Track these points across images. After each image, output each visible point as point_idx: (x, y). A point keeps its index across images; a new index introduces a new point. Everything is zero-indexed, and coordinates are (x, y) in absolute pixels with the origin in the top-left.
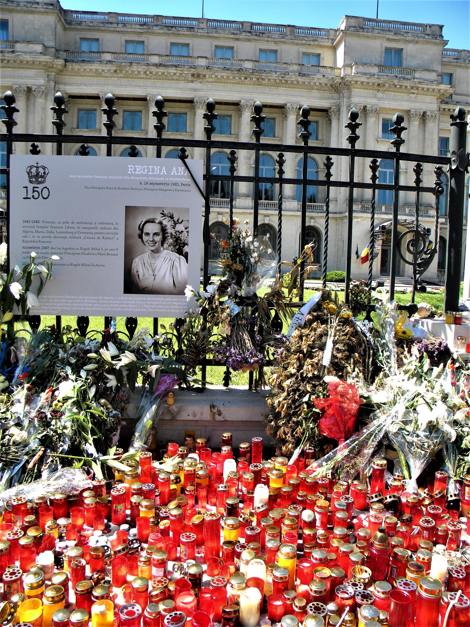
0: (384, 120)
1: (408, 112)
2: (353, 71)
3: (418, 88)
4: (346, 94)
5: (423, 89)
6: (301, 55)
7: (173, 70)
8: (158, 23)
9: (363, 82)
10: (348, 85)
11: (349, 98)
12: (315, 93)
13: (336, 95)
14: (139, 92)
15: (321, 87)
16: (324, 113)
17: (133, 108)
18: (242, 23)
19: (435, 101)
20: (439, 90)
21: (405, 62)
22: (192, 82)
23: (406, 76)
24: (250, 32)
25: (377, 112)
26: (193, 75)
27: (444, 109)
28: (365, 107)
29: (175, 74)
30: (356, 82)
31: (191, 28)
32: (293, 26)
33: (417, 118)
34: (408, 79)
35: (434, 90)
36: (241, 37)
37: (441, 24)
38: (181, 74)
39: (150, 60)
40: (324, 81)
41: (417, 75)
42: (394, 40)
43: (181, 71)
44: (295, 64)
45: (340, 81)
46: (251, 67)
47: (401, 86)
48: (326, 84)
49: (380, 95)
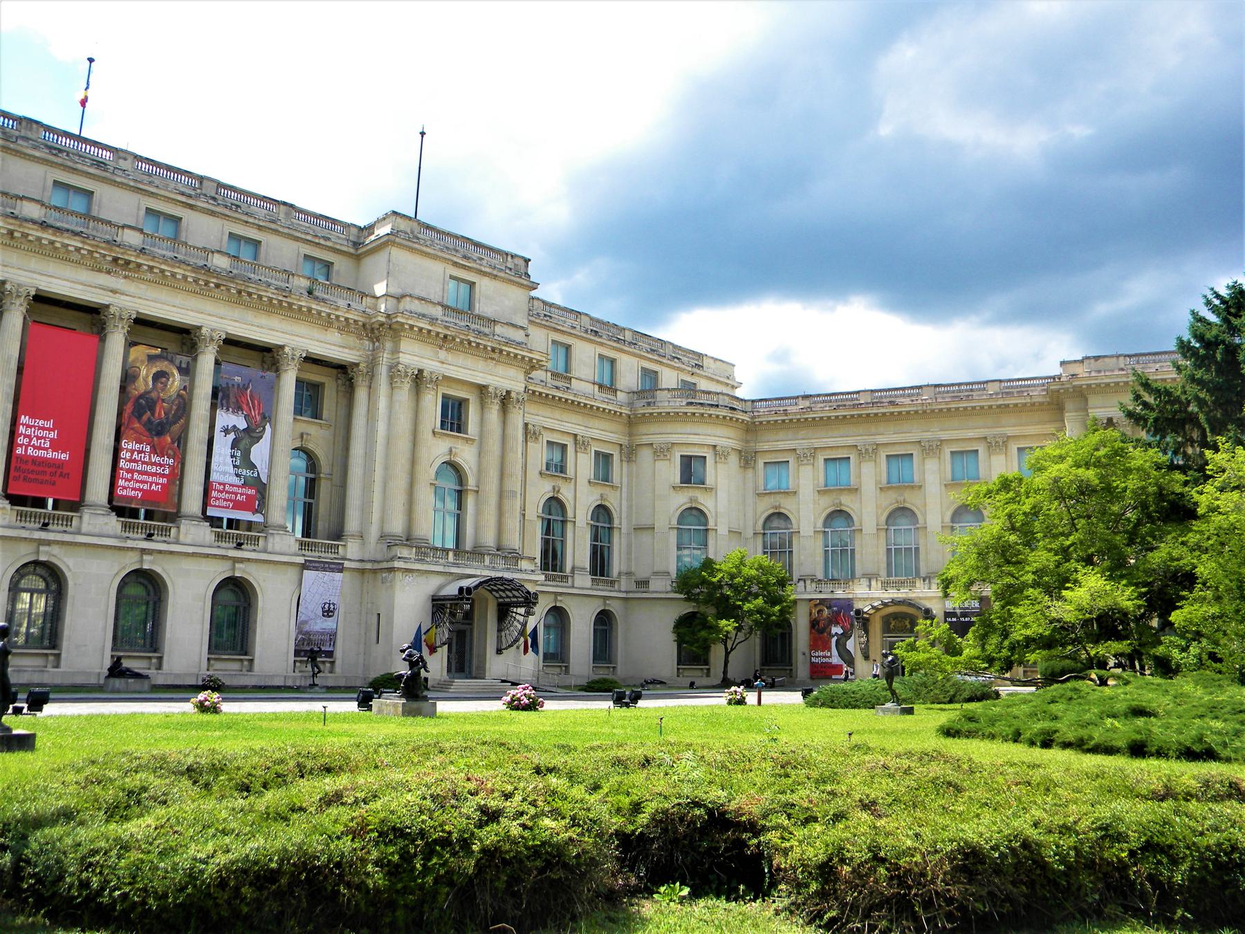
0: (445, 397)
1: (482, 389)
3: (501, 351)
4: (389, 345)
5: (508, 354)
6: (301, 259)
7: (75, 243)
8: (29, 135)
9: (421, 329)
10: (395, 330)
11: (396, 351)
12: (334, 336)
15: (346, 326)
16: (334, 371)
18: (201, 179)
19: (521, 376)
20: (531, 359)
21: (477, 305)
22: (109, 272)
23: (482, 329)
24: (214, 199)
25: (436, 382)
26: (115, 260)
27: (534, 392)
28: (421, 371)
29: (78, 250)
30: (412, 327)
31: (100, 164)
32: (292, 206)
33: (497, 401)
34: (486, 335)
35: (523, 357)
36: (199, 204)
37: (527, 256)
38: (91, 252)
39: (18, 207)
41: (499, 329)
42: (464, 267)
43: (92, 246)
44: (304, 277)
45: (383, 319)
46: (224, 266)
47: (478, 344)
48: (355, 321)
49: (443, 354)
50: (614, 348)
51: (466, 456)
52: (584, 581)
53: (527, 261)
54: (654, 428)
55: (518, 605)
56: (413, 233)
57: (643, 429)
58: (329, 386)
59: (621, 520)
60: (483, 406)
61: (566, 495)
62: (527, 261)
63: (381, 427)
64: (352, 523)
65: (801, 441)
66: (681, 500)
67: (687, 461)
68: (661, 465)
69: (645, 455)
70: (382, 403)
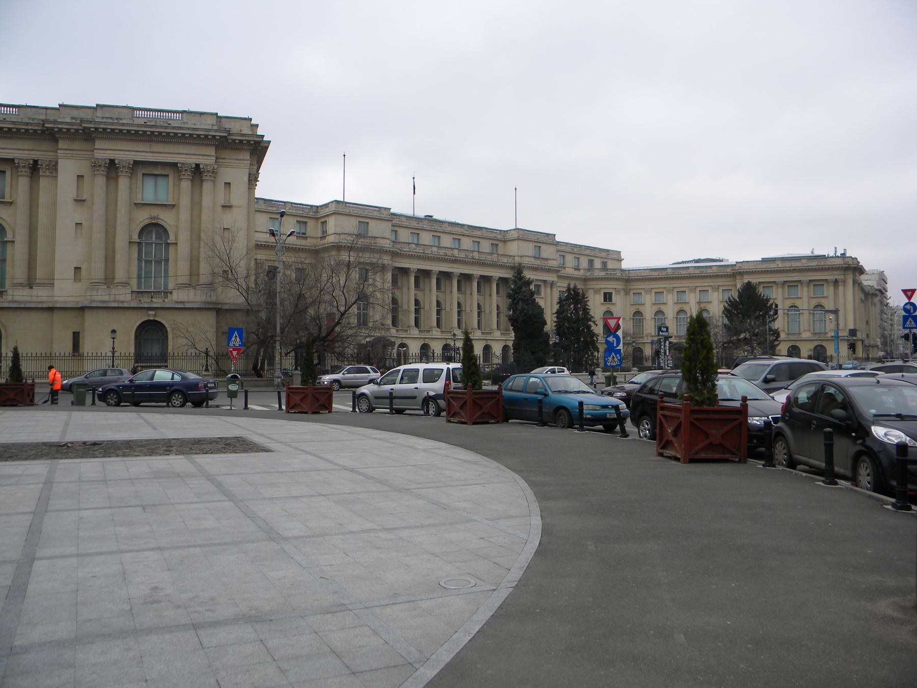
1: (545, 282)
12: (504, 271)
54: (594, 283)
56: (523, 236)
57: (590, 283)
65: (647, 285)
66: (604, 308)
67: (605, 294)
68: (597, 296)
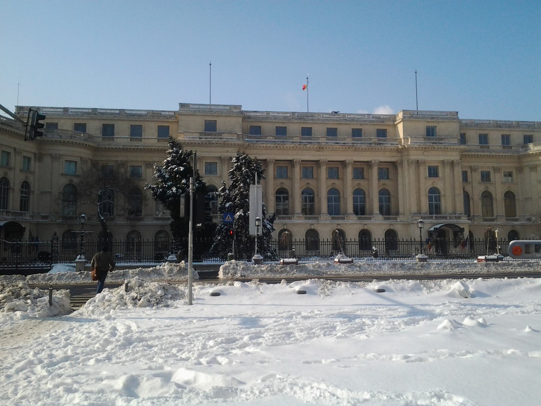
1: (443, 162)
2: (410, 141)
3: (447, 149)
12: (388, 154)
13: (400, 155)
14: (289, 158)
17: (282, 165)
20: (460, 149)
25: (424, 162)
40: (393, 147)
49: (425, 153)
50: (509, 131)
51: (439, 184)
52: (501, 221)
53: (457, 113)
55: (459, 232)
58: (389, 170)
59: (519, 197)
60: (444, 167)
61: (491, 189)
62: (457, 113)
63: (407, 180)
64: (401, 210)
69: (526, 170)
70: (406, 173)
